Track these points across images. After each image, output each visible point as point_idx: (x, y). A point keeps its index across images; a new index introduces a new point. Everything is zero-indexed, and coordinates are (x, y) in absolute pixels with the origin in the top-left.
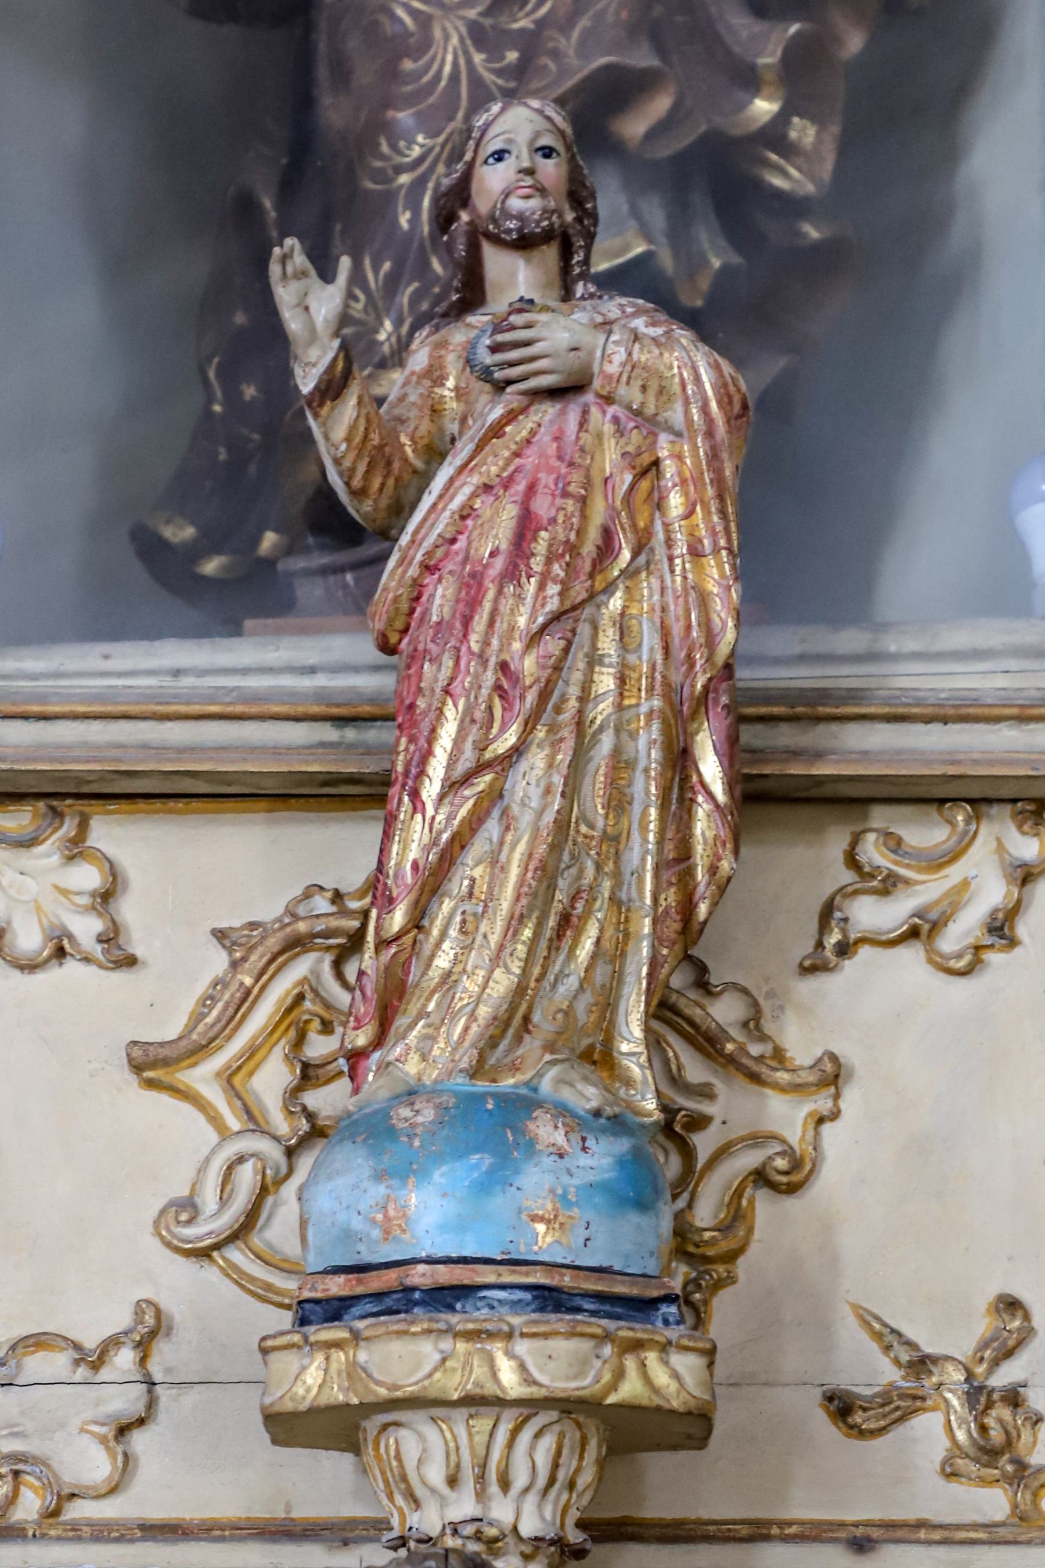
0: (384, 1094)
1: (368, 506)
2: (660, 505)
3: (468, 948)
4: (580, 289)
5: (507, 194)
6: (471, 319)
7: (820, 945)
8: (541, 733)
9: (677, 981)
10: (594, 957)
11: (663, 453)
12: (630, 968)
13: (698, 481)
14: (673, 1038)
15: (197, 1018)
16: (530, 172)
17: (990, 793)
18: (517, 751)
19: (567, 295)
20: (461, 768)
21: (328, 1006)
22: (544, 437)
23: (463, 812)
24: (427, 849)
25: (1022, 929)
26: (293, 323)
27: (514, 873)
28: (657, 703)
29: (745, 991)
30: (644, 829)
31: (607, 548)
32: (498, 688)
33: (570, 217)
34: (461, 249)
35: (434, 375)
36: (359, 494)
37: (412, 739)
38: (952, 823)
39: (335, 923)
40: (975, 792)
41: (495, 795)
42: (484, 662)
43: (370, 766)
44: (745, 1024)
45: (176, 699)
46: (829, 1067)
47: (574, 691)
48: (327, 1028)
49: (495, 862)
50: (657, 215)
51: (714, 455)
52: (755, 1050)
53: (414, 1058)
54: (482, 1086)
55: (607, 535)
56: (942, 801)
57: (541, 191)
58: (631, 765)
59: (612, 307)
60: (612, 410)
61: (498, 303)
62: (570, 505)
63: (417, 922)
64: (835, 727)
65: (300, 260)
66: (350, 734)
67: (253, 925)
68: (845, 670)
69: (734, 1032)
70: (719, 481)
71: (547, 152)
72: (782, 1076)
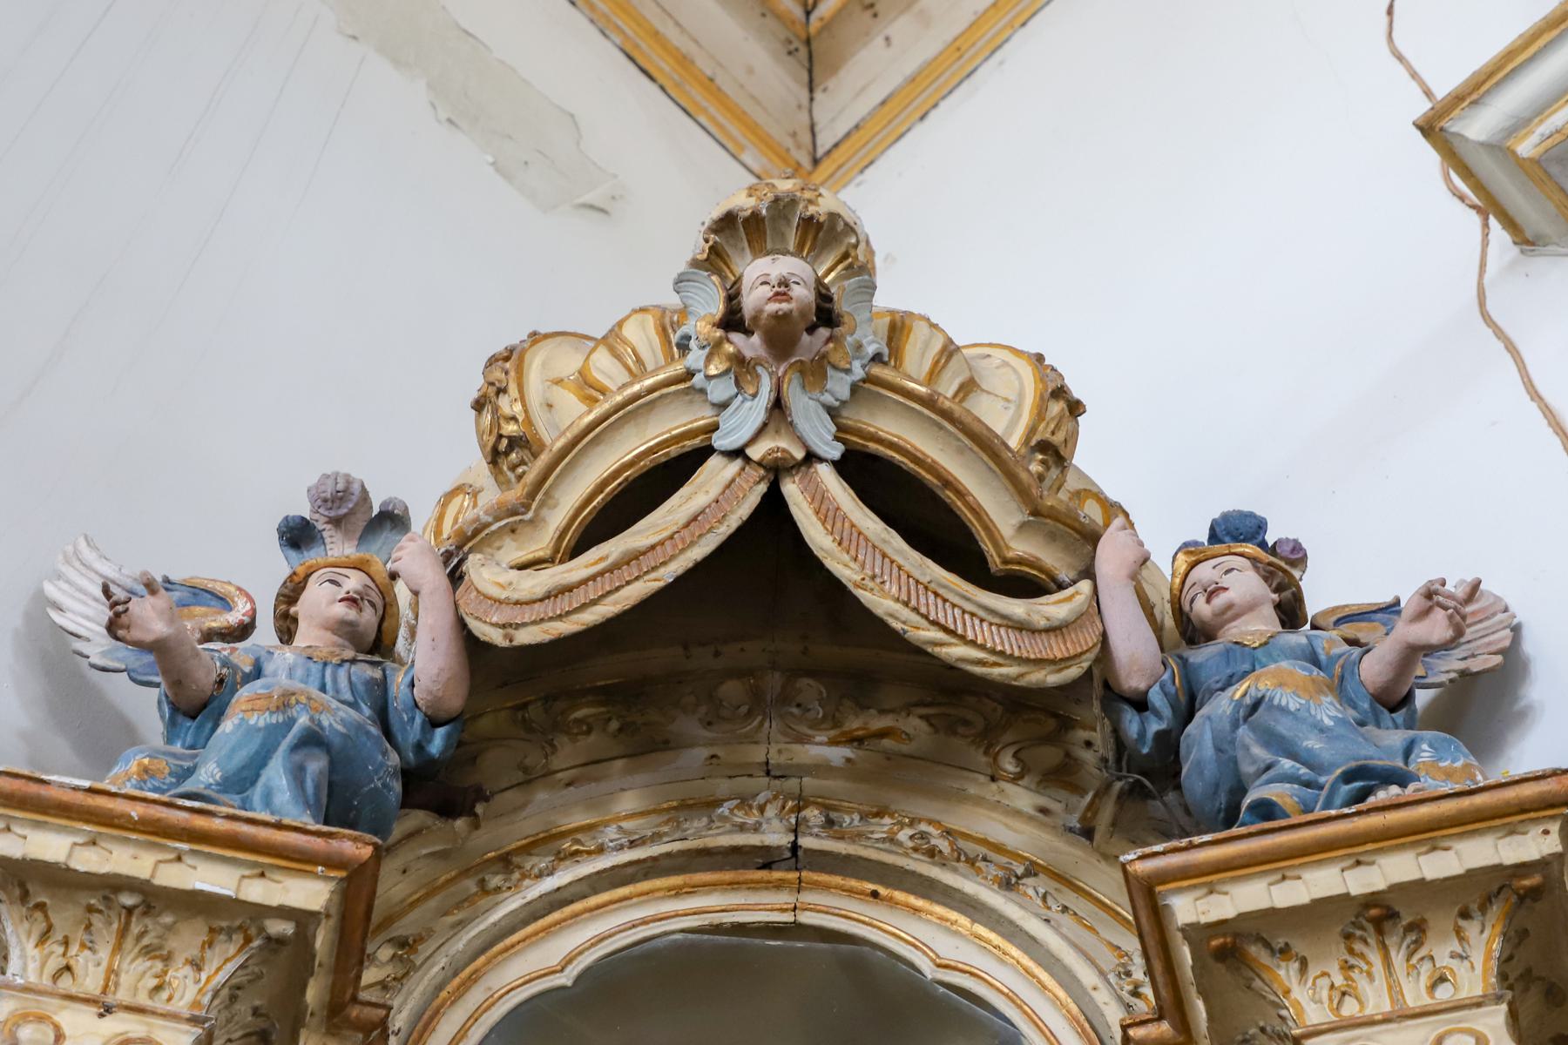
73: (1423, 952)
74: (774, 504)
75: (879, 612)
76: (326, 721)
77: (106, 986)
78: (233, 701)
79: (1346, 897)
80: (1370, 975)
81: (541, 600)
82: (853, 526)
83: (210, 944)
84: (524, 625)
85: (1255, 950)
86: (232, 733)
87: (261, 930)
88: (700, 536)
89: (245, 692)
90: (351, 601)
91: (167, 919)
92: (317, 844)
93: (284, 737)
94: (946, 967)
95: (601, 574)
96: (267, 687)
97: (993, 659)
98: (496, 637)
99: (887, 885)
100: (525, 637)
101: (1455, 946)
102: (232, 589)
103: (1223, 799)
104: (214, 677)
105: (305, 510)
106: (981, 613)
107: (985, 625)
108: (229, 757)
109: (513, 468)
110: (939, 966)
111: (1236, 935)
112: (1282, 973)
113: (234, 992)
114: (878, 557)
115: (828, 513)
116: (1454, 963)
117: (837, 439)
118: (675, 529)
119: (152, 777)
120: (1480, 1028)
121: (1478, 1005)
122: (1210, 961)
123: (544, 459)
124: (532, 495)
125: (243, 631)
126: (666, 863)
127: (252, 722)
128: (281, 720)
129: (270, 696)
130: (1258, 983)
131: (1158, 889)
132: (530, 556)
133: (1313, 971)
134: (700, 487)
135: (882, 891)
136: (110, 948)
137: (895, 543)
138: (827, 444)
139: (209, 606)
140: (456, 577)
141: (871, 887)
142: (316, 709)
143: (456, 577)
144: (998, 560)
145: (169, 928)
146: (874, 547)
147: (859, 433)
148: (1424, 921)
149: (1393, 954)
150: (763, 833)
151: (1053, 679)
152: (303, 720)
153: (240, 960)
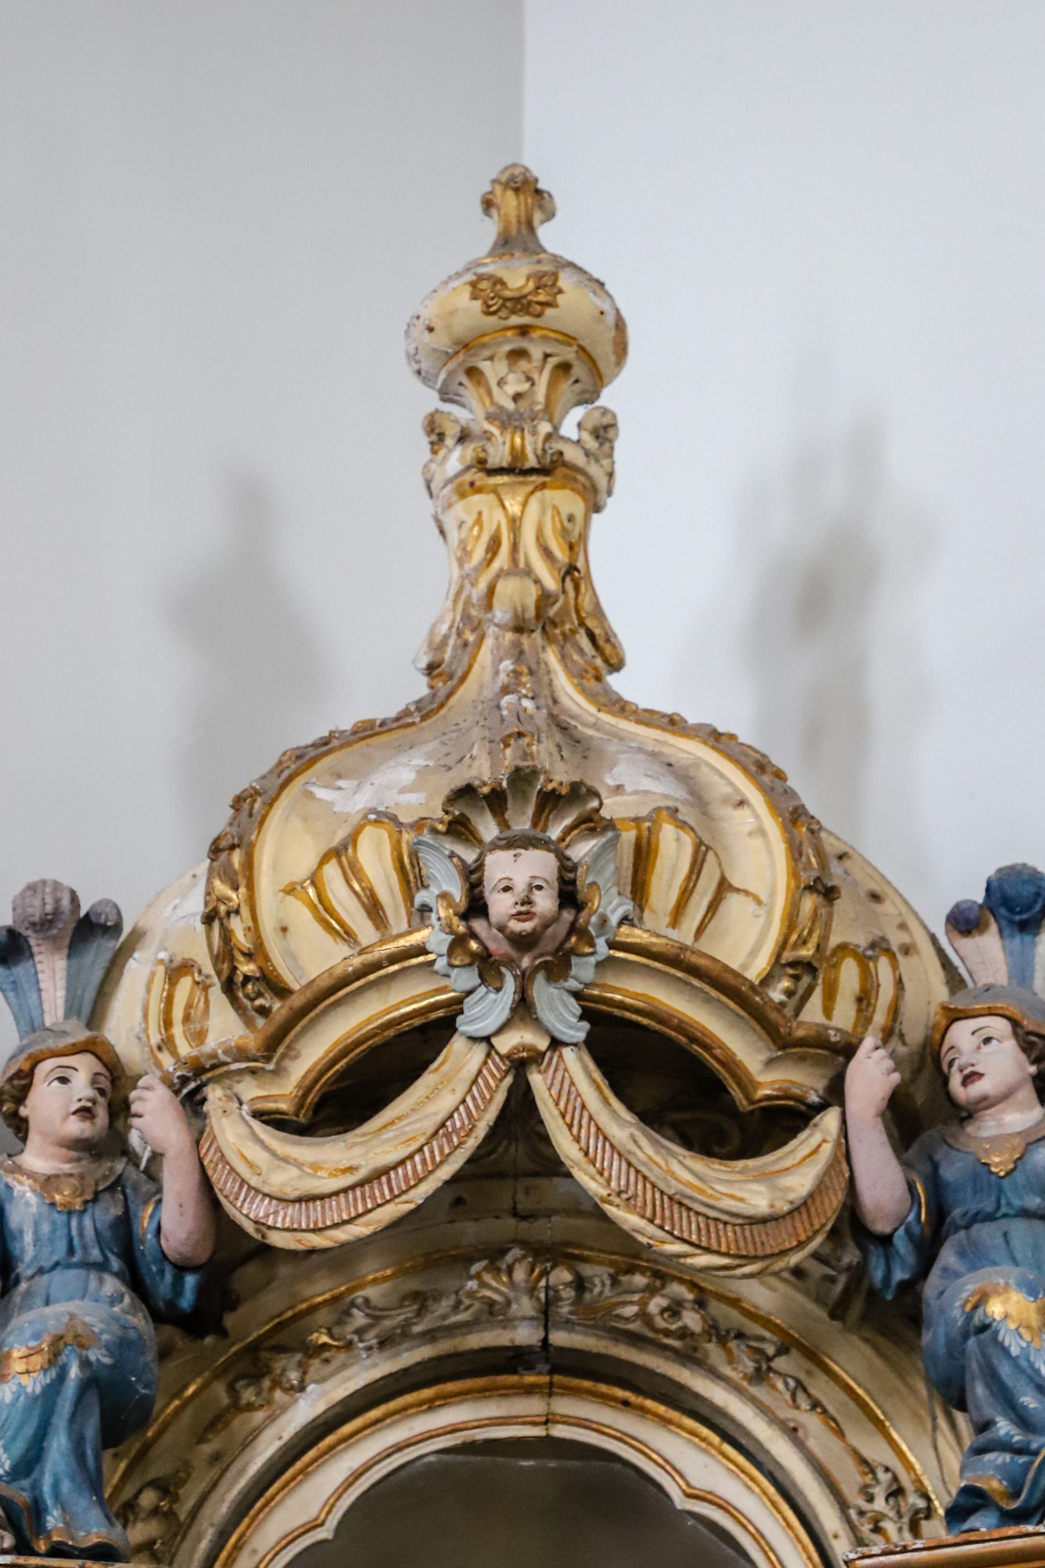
82: (598, 1129)
97: (737, 1262)
106: (725, 1217)
107: (729, 1228)
117: (582, 1018)
118: (422, 1140)
138: (571, 1027)
144: (745, 1102)
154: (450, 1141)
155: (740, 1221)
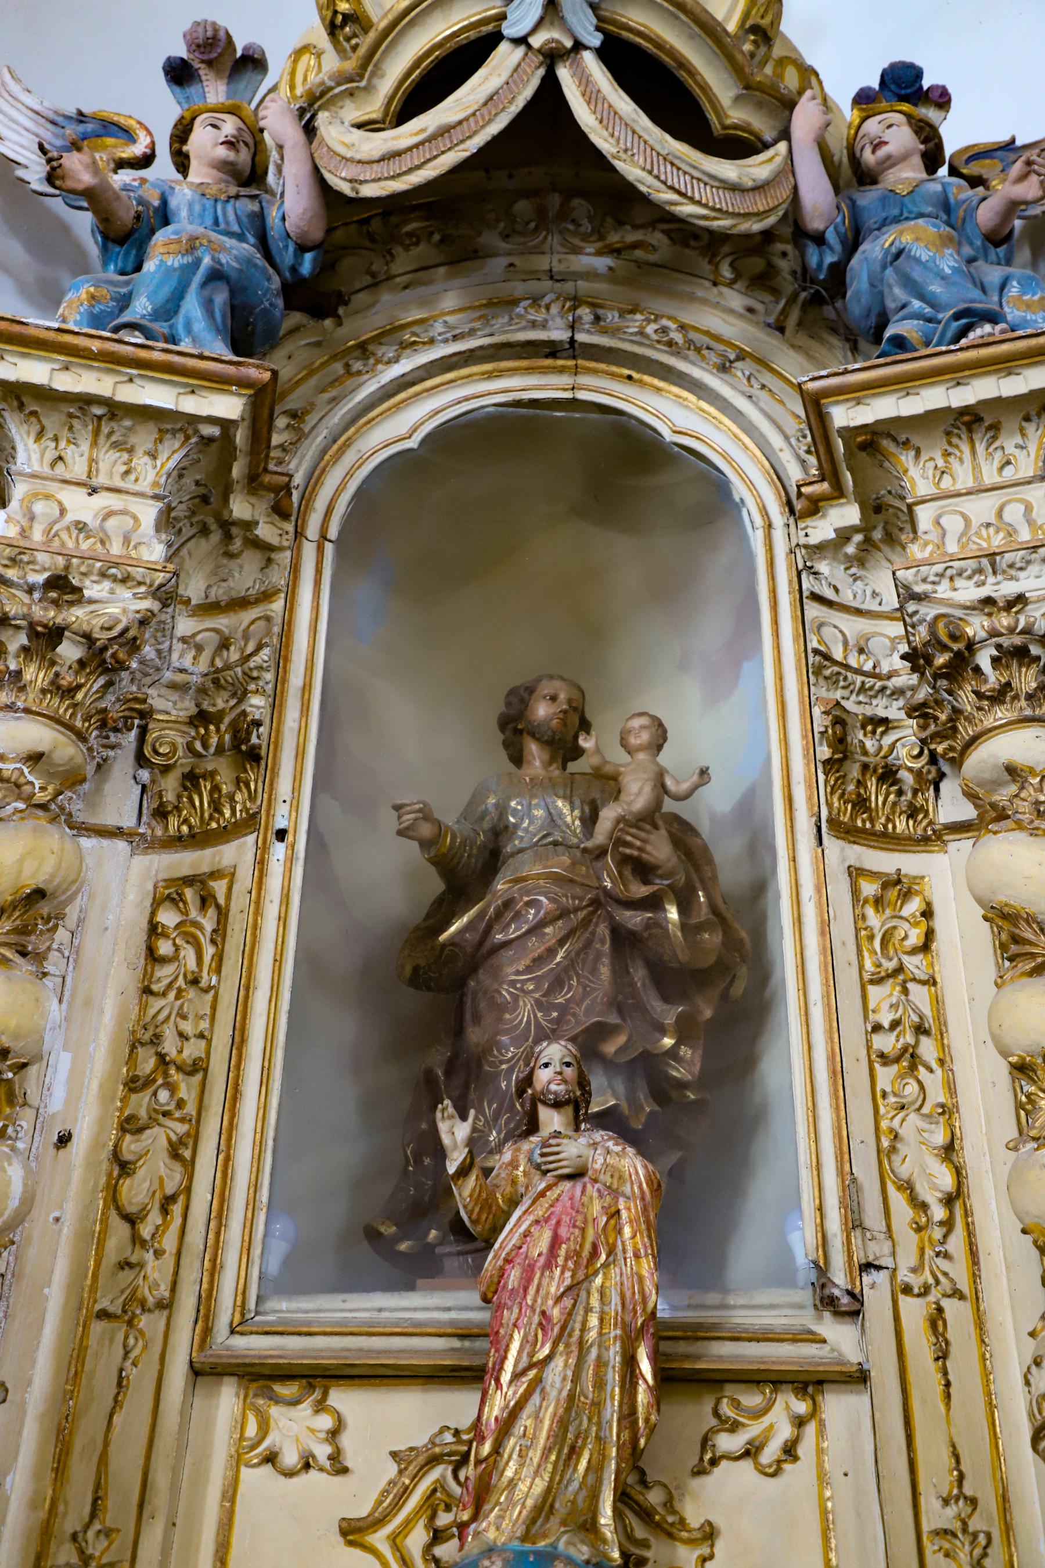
0: (476, 1551)
1: (479, 1228)
2: (620, 1232)
3: (522, 1465)
4: (583, 1126)
5: (549, 1083)
6: (532, 1139)
7: (701, 1459)
8: (561, 1347)
9: (630, 1480)
10: (587, 1469)
11: (621, 1207)
12: (606, 1476)
13: (638, 1221)
14: (628, 1513)
15: (379, 1503)
16: (560, 1073)
17: (781, 1378)
18: (549, 1358)
19: (577, 1129)
20: (521, 1367)
21: (449, 1495)
22: (565, 1198)
23: (521, 1390)
24: (503, 1410)
25: (800, 1451)
26: (446, 1140)
27: (547, 1423)
28: (619, 1332)
29: (665, 1486)
30: (612, 1398)
31: (594, 1254)
32: (540, 1324)
33: (578, 1093)
34: (528, 1105)
35: (514, 1164)
36: (475, 1222)
37: (497, 1351)
38: (764, 1393)
39: (454, 1448)
40: (773, 1378)
41: (538, 1381)
42: (534, 1311)
43: (476, 1362)
44: (665, 1505)
45: (379, 1324)
46: (707, 1529)
47: (578, 1326)
48: (448, 1508)
49: (537, 1417)
50: (621, 1088)
51: (645, 1210)
52: (670, 1519)
53: (492, 1529)
54: (528, 1546)
55: (595, 1247)
56: (758, 1382)
57: (565, 1081)
58: (606, 1364)
59: (598, 1135)
60: (597, 1186)
61: (545, 1131)
62: (577, 1231)
63: (497, 1450)
64: (705, 1343)
65: (451, 1110)
66: (467, 1344)
67: (411, 1449)
68: (709, 1313)
69: (659, 1509)
70: (648, 1222)
71: (568, 1064)
72: (684, 1535)
73: (997, 444)
74: (550, 86)
75: (631, 178)
76: (224, 259)
77: (90, 471)
78: (153, 242)
79: (949, 408)
80: (961, 460)
81: (378, 161)
82: (610, 106)
83: (161, 441)
84: (366, 181)
85: (886, 444)
86: (155, 272)
87: (196, 431)
88: (496, 115)
89: (161, 236)
90: (229, 144)
91: (127, 423)
92: (231, 370)
93: (194, 274)
94: (680, 433)
95: (422, 143)
96: (176, 233)
98: (345, 188)
99: (638, 372)
100: (368, 191)
101: (1019, 440)
102: (133, 123)
103: (873, 320)
104: (132, 213)
105: (181, 51)
108: (155, 293)
109: (348, 39)
110: (675, 432)
111: (874, 433)
112: (903, 458)
113: (181, 472)
114: (630, 133)
115: (592, 96)
116: (1017, 452)
117: (598, 29)
119: (99, 302)
120: (1028, 498)
121: (1029, 483)
122: (856, 450)
123: (372, 35)
124: (364, 66)
125: (146, 161)
126: (479, 353)
127: (169, 263)
128: (190, 259)
129: (179, 242)
130: (887, 464)
131: (823, 401)
132: (366, 118)
133: (924, 457)
134: (494, 69)
135: (635, 375)
136: (88, 443)
137: (643, 122)
138: (590, 34)
139: (117, 137)
140: (310, 130)
141: (627, 372)
142: (215, 250)
143: (310, 130)
145: (129, 429)
146: (626, 125)
147: (614, 23)
148: (1000, 422)
149: (977, 445)
150: (549, 330)
151: (756, 227)
152: (207, 261)
153: (183, 452)
154: (496, 106)
155: (716, 184)
